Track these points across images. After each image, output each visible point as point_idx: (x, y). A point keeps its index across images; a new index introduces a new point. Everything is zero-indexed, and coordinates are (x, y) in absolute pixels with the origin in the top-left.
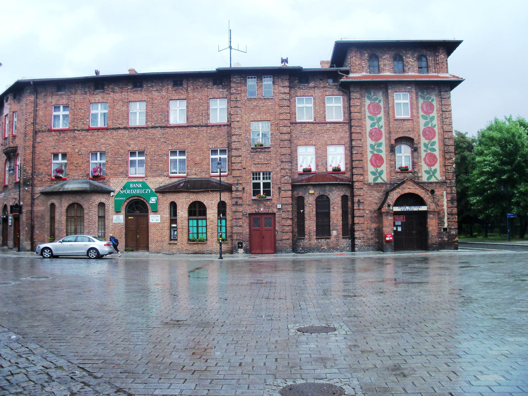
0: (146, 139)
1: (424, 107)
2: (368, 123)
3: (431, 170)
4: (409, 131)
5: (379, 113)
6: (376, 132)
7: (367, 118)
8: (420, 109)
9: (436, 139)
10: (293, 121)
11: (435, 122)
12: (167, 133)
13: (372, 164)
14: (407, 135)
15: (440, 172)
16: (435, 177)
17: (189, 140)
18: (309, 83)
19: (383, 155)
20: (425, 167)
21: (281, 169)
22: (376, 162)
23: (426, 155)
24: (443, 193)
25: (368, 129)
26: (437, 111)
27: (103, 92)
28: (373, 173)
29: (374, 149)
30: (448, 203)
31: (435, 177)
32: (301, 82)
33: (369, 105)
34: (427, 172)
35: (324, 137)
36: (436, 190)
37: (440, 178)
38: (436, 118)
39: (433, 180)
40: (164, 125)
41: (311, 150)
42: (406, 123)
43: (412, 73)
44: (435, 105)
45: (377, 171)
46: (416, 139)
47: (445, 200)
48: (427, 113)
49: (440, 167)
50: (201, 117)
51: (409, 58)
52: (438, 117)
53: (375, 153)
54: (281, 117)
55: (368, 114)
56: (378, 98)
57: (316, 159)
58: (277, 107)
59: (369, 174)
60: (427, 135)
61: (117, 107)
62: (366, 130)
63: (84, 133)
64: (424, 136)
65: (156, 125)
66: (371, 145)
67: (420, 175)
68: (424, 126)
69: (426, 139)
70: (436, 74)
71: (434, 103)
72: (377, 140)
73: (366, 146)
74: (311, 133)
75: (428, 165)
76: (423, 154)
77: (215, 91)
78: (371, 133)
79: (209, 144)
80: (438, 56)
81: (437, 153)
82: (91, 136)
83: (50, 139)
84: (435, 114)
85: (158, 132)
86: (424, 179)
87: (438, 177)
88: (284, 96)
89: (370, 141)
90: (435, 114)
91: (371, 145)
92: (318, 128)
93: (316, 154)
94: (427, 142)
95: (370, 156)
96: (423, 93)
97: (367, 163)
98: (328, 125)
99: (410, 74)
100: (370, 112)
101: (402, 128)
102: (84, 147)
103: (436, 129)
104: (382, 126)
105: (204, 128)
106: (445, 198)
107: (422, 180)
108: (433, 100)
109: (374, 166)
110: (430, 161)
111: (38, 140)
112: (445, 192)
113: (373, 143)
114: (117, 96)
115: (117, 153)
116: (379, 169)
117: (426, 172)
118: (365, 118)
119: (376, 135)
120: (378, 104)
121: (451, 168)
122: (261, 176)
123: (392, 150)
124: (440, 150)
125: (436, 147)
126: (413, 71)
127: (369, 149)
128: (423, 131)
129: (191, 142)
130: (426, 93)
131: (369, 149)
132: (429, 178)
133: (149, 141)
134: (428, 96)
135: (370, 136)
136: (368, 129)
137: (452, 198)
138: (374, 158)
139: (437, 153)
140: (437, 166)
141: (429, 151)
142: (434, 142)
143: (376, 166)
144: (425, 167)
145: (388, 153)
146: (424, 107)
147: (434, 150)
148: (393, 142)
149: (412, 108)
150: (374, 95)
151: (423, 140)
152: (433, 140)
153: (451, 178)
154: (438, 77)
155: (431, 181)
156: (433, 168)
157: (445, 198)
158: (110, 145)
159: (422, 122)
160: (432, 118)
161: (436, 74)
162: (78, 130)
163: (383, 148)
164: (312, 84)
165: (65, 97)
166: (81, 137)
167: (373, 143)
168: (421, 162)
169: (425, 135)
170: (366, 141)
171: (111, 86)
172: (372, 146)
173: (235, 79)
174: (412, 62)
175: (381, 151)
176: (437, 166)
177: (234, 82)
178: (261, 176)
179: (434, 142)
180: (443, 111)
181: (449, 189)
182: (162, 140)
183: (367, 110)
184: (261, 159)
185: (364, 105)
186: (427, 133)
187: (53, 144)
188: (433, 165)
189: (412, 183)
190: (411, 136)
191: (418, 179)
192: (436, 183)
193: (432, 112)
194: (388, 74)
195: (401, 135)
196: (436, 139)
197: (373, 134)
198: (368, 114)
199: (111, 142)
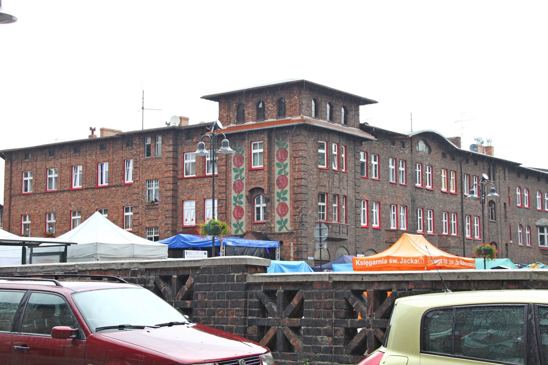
0: (82, 200)
1: (279, 154)
2: (233, 174)
3: (282, 221)
4: (260, 181)
5: (242, 165)
6: (239, 184)
7: (232, 170)
8: (276, 157)
9: (288, 188)
10: (180, 176)
11: (288, 169)
12: (95, 194)
13: (235, 216)
14: (258, 186)
15: (291, 222)
16: (286, 228)
17: (110, 199)
18: (193, 139)
19: (243, 206)
20: (277, 218)
21: (166, 224)
22: (238, 215)
23: (278, 205)
24: (290, 244)
25: (233, 181)
26: (290, 157)
27: (54, 158)
28: (234, 225)
29: (236, 202)
30: (294, 255)
31: (286, 228)
32: (188, 138)
33: (234, 157)
34: (279, 222)
35: (202, 191)
36: (284, 241)
37: (290, 229)
38: (289, 164)
39: (284, 230)
40: (93, 186)
41: (193, 203)
42: (258, 173)
43: (271, 121)
44: (289, 151)
45: (238, 223)
46: (266, 189)
47: (292, 251)
48: (282, 160)
49: (291, 216)
50: (118, 178)
51: (269, 103)
52: (291, 163)
53: (237, 205)
54: (166, 175)
55: (233, 166)
56: (241, 149)
57: (196, 212)
58: (164, 166)
59: (232, 226)
60: (280, 184)
61: (64, 172)
62: (231, 182)
63: (42, 196)
64: (277, 185)
65: (89, 187)
66: (234, 197)
67: (273, 225)
68: (278, 174)
69: (279, 188)
70: (290, 118)
71: (288, 149)
72: (239, 192)
73: (231, 198)
74: (193, 188)
75: (280, 215)
76: (276, 204)
77: (126, 153)
78: (234, 185)
79: (122, 202)
80: (292, 97)
81: (288, 202)
82: (47, 198)
83: (20, 202)
84: (288, 161)
85: (89, 193)
86: (277, 230)
87: (289, 227)
88: (168, 154)
89: (234, 194)
90: (288, 161)
91: (234, 197)
92: (198, 183)
93: (196, 207)
94: (279, 191)
95: (233, 207)
96: (278, 139)
97: (231, 216)
98: (206, 180)
99: (269, 120)
100: (235, 164)
101: (255, 179)
102: (42, 209)
103: (288, 177)
104: (244, 177)
105: (119, 188)
106: (292, 249)
107: (274, 231)
108: (287, 146)
109: (236, 218)
110: (282, 211)
111: (12, 203)
112: (292, 243)
113: (236, 195)
114: (64, 161)
115: (63, 214)
116: (240, 221)
117: (279, 222)
118: (231, 170)
119: (238, 187)
120: (241, 155)
121: (298, 218)
122: (154, 231)
123: (250, 201)
124: (291, 199)
125: (288, 196)
126: (272, 117)
127: (233, 202)
128: (277, 180)
129: (110, 202)
130: (281, 139)
131: (233, 202)
132: (280, 229)
133: (84, 202)
134: (283, 142)
135: (234, 190)
136: (233, 181)
137: (298, 249)
138: (236, 211)
139: (288, 202)
140: (288, 216)
141: (281, 201)
142: (286, 191)
143: (238, 218)
144: (277, 218)
145: (247, 205)
146: (279, 154)
147: (286, 199)
148: (248, 193)
149: (264, 158)
150: (239, 146)
151: (277, 190)
152: (285, 189)
153: (297, 228)
154: (289, 121)
155: (282, 232)
156: (284, 218)
157: (292, 249)
158: (58, 206)
159: (277, 170)
160: (286, 166)
161: (290, 118)
162: (38, 194)
163: (244, 200)
164: (195, 140)
165: (30, 164)
166: (40, 200)
167: (236, 195)
168: (274, 212)
169: (278, 184)
170: (231, 194)
171: (60, 153)
172: (235, 198)
173: (136, 141)
174: (271, 107)
175: (242, 203)
176: (288, 216)
177: (136, 144)
178: (154, 231)
179: (286, 191)
180: (294, 158)
181: (295, 240)
182: (92, 200)
183: (232, 162)
184: (152, 215)
185: (231, 157)
186: (280, 181)
187: (22, 206)
188: (285, 215)
189: (251, 235)
190: (262, 186)
191: (271, 230)
192: (285, 233)
193: (286, 159)
194: (251, 123)
195: (253, 186)
196: (288, 188)
197: (237, 185)
198: (233, 166)
199: (60, 203)
